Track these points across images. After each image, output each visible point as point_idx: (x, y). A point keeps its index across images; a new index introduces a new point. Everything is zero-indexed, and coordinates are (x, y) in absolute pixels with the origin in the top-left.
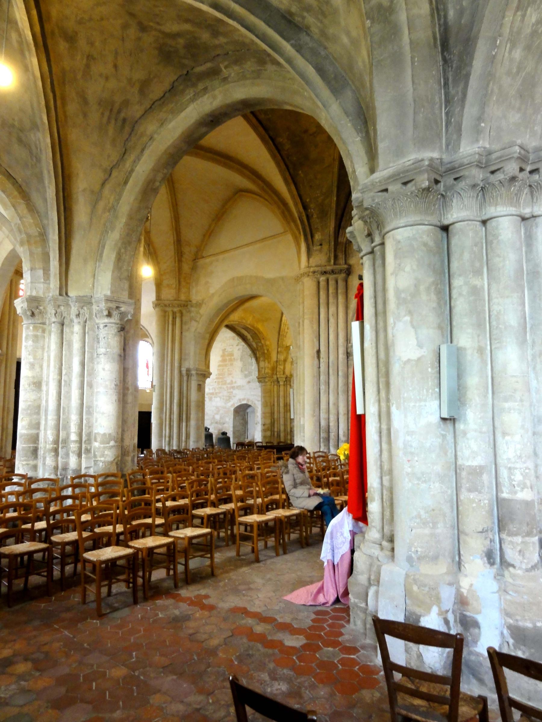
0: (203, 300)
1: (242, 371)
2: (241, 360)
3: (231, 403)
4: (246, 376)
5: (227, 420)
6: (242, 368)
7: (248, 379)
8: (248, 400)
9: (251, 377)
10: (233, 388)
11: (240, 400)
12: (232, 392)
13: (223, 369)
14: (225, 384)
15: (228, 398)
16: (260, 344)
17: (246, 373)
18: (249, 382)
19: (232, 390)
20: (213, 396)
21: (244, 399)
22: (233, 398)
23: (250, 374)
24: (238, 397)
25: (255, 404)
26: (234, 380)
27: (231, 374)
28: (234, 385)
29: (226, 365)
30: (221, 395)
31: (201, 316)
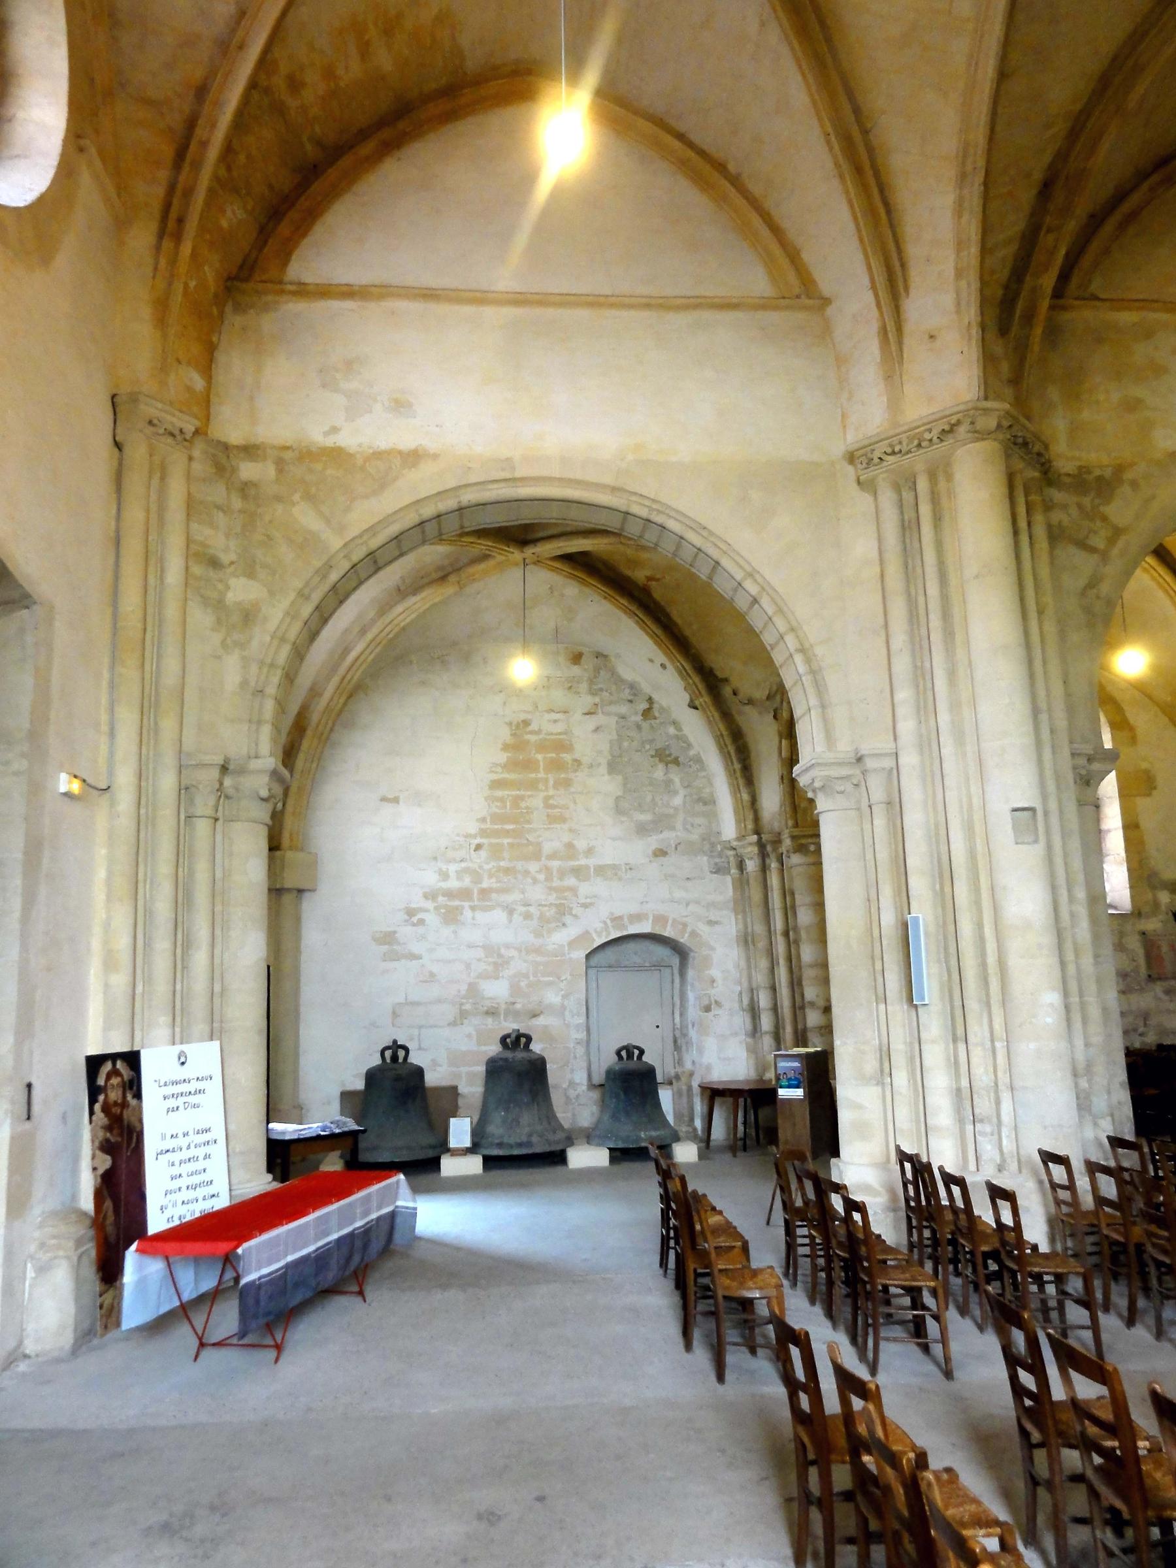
0: (1119, 469)
1: (619, 811)
2: (612, 768)
3: (572, 931)
4: (642, 830)
5: (552, 997)
7: (654, 841)
8: (660, 919)
9: (666, 834)
10: (579, 872)
11: (617, 920)
12: (574, 890)
13: (517, 800)
14: (537, 856)
15: (550, 912)
17: (645, 817)
18: (660, 853)
19: (571, 881)
20: (466, 904)
21: (637, 918)
23: (661, 822)
24: (604, 911)
25: (693, 934)
26: (581, 844)
27: (562, 819)
28: (583, 862)
29: (533, 785)
31: (1117, 532)
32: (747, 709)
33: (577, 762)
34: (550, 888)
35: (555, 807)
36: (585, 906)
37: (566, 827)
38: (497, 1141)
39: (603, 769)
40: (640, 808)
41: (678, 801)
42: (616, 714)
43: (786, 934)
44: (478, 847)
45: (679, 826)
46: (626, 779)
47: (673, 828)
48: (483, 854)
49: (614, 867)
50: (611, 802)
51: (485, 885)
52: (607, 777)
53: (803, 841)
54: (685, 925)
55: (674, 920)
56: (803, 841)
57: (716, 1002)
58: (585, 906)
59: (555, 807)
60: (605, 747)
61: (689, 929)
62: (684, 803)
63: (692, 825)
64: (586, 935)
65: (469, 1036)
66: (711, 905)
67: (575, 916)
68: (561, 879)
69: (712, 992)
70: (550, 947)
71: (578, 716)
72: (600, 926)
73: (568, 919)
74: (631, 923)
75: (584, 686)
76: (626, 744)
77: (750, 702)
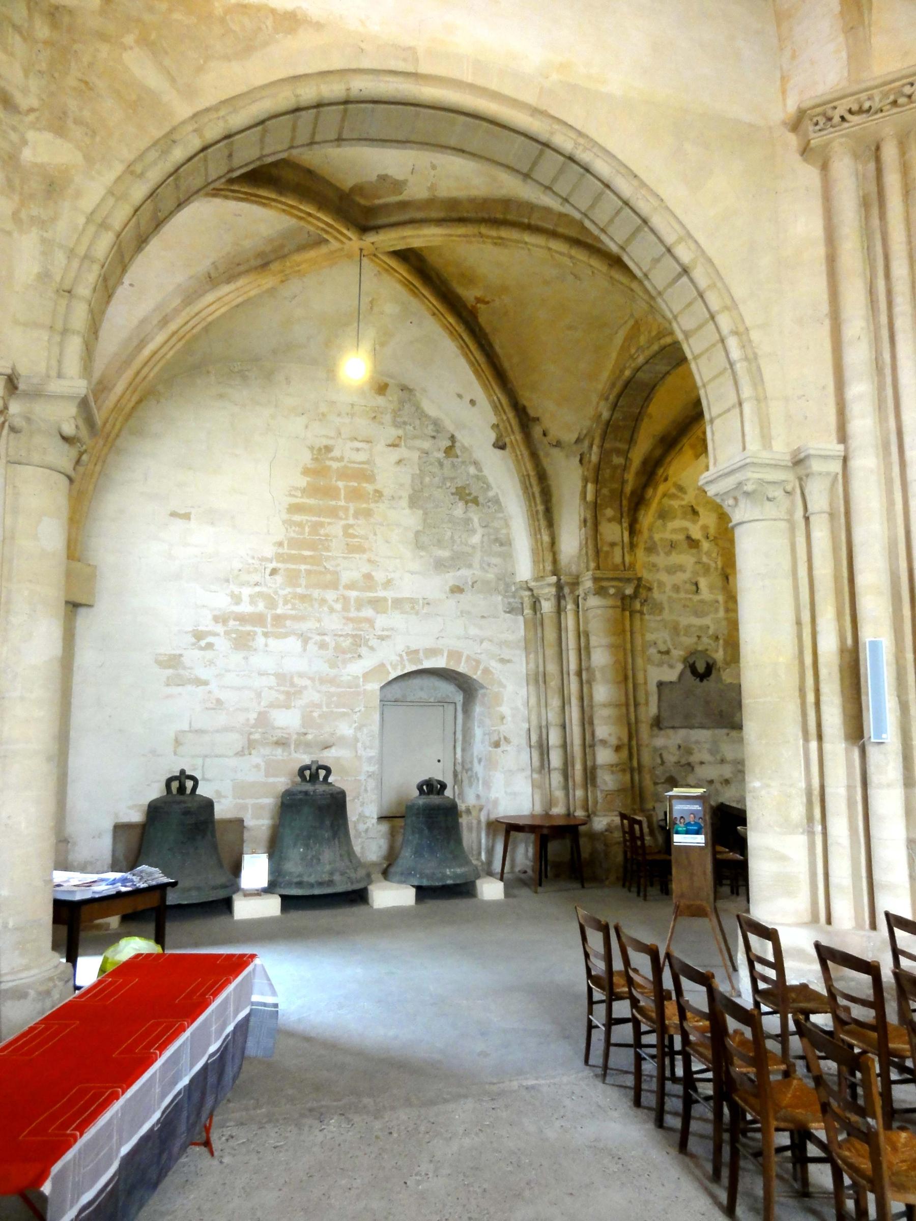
1: (419, 545)
2: (414, 502)
3: (368, 662)
4: (440, 565)
5: (345, 729)
6: (417, 533)
7: (451, 578)
8: (454, 655)
9: (465, 572)
11: (413, 654)
12: (370, 622)
13: (316, 527)
14: (334, 585)
15: (346, 643)
16: (618, 460)
17: (445, 554)
18: (457, 590)
19: (368, 612)
20: (259, 630)
21: (432, 652)
22: (373, 642)
23: (458, 560)
24: (400, 644)
25: (486, 671)
26: (379, 576)
27: (360, 549)
28: (381, 594)
29: (333, 513)
30: (309, 625)
32: (555, 452)
33: (379, 494)
34: (348, 619)
35: (354, 536)
36: (382, 638)
37: (365, 556)
38: (295, 880)
39: (404, 503)
40: (439, 543)
41: (476, 539)
42: (418, 449)
43: (579, 674)
44: (274, 572)
45: (476, 565)
46: (425, 514)
47: (470, 566)
48: (279, 578)
49: (413, 601)
50: (411, 535)
51: (279, 611)
52: (407, 511)
53: (605, 584)
54: (478, 662)
55: (468, 657)
56: (605, 584)
57: (505, 738)
58: (382, 638)
59: (354, 536)
60: (407, 480)
61: (481, 667)
62: (482, 542)
63: (489, 565)
64: (381, 668)
65: (257, 766)
66: (503, 644)
67: (372, 649)
68: (358, 609)
69: (502, 728)
70: (345, 678)
71: (380, 447)
72: (394, 658)
73: (364, 651)
74: (427, 658)
75: (388, 418)
76: (427, 479)
77: (558, 444)
